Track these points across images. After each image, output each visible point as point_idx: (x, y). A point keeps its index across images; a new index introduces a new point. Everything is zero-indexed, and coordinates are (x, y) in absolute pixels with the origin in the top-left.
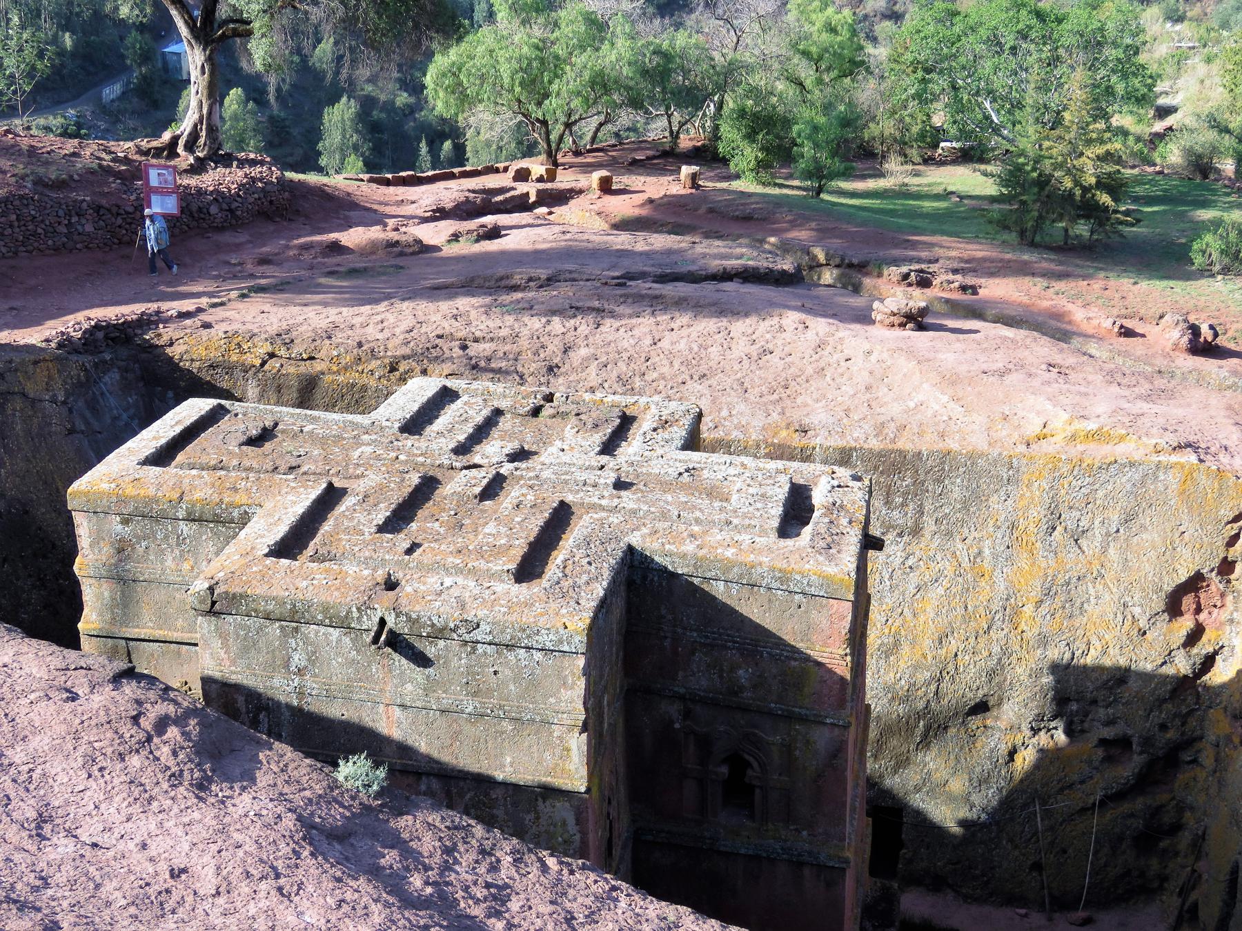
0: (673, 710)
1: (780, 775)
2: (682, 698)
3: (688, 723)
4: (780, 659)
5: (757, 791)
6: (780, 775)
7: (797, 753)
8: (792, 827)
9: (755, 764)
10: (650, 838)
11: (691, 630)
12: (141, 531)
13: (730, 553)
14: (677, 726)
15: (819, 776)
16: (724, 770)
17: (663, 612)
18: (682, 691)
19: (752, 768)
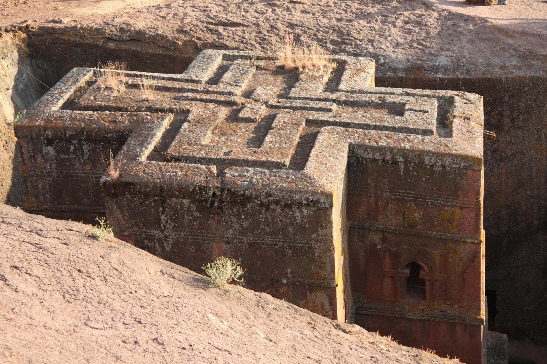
0: (375, 238)
1: (440, 273)
2: (382, 231)
3: (385, 245)
4: (439, 206)
5: (427, 283)
6: (440, 273)
7: (450, 260)
8: (449, 303)
9: (425, 267)
10: (365, 312)
11: (386, 192)
12: (60, 148)
13: (407, 146)
14: (379, 247)
15: (463, 273)
16: (407, 271)
17: (369, 182)
18: (382, 227)
19: (424, 269)
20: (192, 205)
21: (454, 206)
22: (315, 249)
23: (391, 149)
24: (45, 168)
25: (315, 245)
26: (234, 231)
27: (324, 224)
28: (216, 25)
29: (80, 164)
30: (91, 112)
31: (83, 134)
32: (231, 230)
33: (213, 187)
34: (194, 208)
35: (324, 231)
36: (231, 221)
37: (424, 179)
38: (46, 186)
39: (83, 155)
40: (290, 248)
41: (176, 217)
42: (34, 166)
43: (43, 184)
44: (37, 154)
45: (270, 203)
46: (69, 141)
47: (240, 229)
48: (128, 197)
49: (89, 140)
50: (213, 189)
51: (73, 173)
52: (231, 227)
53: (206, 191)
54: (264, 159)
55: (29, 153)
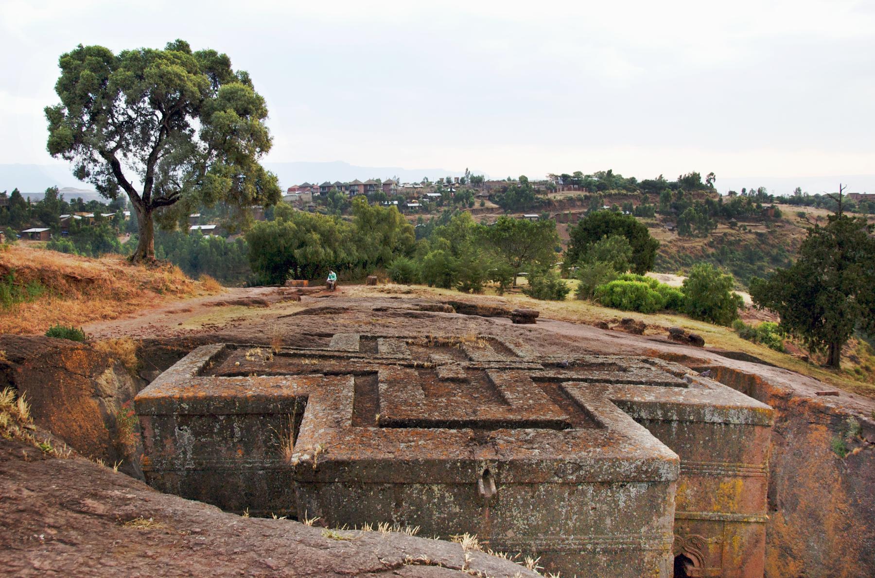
12: (199, 427)
20: (447, 494)
21: (735, 476)
22: (644, 550)
23: (663, 406)
24: (177, 458)
25: (645, 544)
26: (515, 532)
27: (661, 510)
28: (312, 336)
29: (228, 449)
30: (240, 378)
31: (234, 404)
32: (510, 531)
33: (486, 460)
34: (449, 498)
35: (661, 519)
36: (511, 516)
37: (701, 442)
38: (177, 484)
39: (232, 436)
40: (605, 551)
41: (419, 516)
42: (160, 456)
43: (172, 482)
44: (167, 438)
45: (578, 482)
46: (214, 417)
47: (525, 528)
48: (338, 487)
49: (243, 415)
50: (486, 464)
51: (217, 463)
52: (511, 526)
53: (473, 468)
54: (533, 417)
55: (155, 437)
